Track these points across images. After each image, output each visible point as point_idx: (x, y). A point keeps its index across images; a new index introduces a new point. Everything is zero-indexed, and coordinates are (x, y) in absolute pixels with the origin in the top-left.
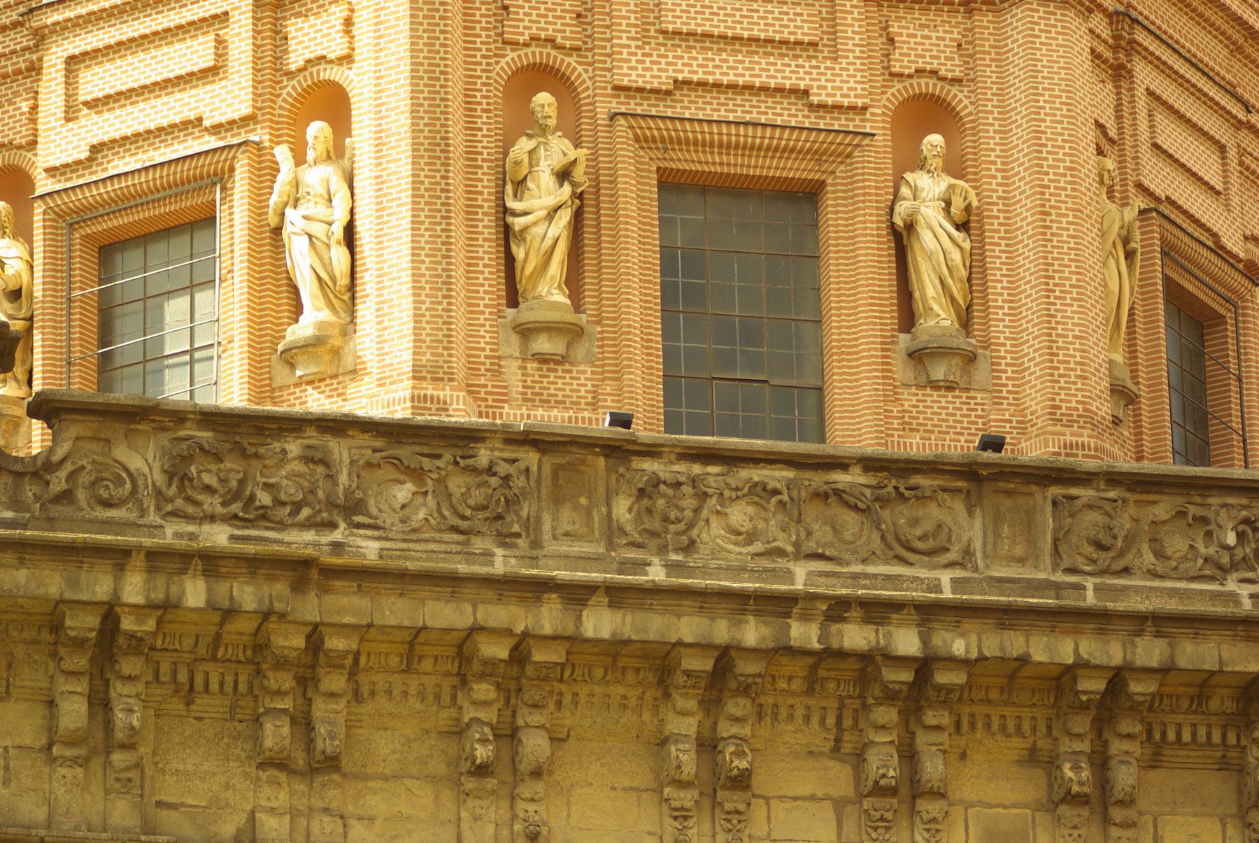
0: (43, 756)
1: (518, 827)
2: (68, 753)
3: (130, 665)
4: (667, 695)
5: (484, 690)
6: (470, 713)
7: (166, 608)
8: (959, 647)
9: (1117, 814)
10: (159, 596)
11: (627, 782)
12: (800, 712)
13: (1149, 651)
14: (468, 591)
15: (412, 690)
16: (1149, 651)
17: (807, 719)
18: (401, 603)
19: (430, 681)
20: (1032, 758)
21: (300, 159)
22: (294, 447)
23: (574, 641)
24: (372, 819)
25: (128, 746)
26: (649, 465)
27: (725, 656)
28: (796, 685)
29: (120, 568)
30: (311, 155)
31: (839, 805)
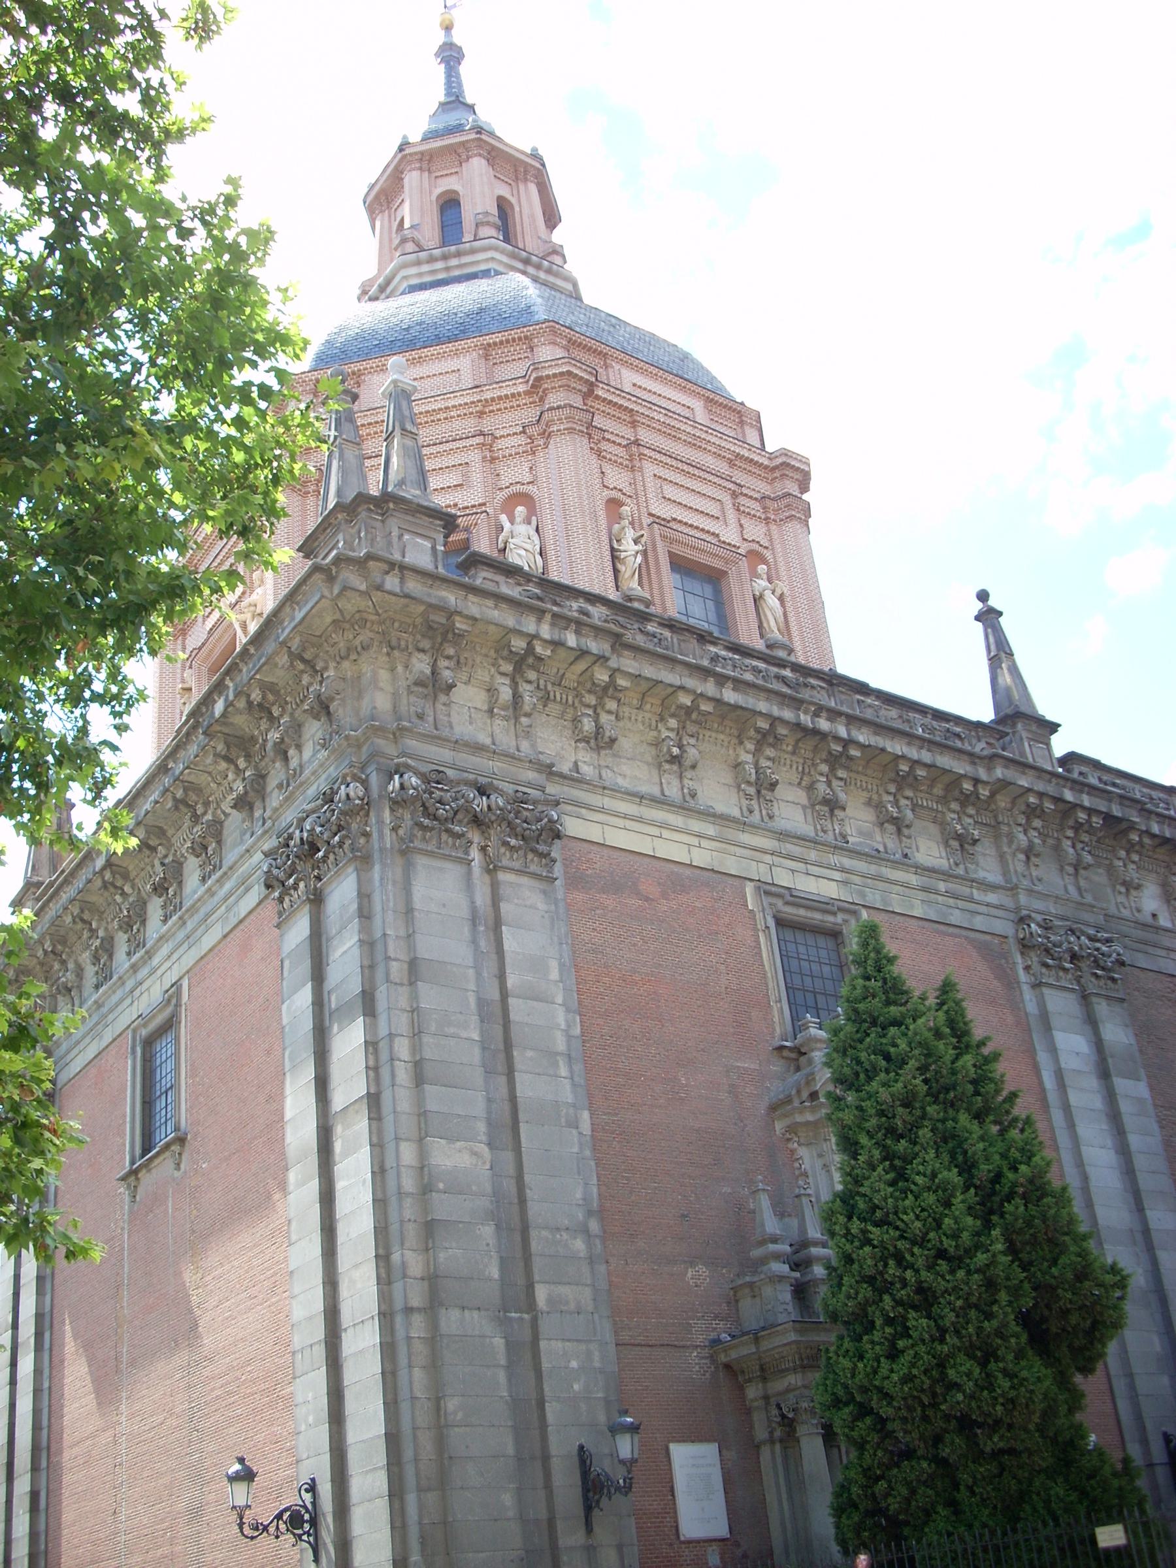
0: (486, 715)
1: (686, 791)
2: (502, 713)
3: (532, 675)
4: (741, 743)
5: (673, 723)
6: (665, 734)
7: (557, 644)
8: (861, 739)
9: (906, 831)
10: (556, 637)
11: (726, 782)
12: (788, 762)
13: (926, 756)
14: (679, 668)
15: (640, 719)
16: (926, 756)
17: (791, 766)
18: (651, 669)
19: (648, 715)
20: (869, 803)
21: (512, 522)
22: (575, 605)
23: (718, 702)
24: (625, 776)
25: (528, 715)
26: (713, 649)
27: (774, 721)
28: (790, 748)
29: (539, 620)
30: (518, 520)
31: (804, 807)
